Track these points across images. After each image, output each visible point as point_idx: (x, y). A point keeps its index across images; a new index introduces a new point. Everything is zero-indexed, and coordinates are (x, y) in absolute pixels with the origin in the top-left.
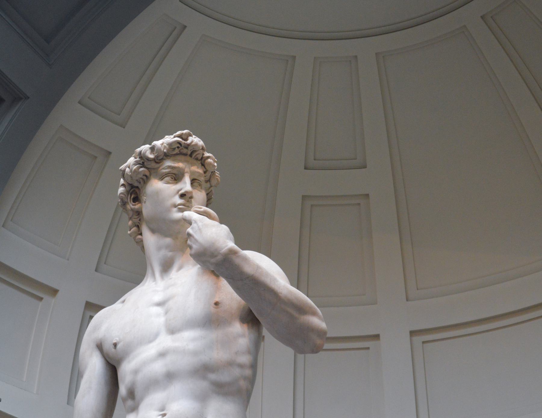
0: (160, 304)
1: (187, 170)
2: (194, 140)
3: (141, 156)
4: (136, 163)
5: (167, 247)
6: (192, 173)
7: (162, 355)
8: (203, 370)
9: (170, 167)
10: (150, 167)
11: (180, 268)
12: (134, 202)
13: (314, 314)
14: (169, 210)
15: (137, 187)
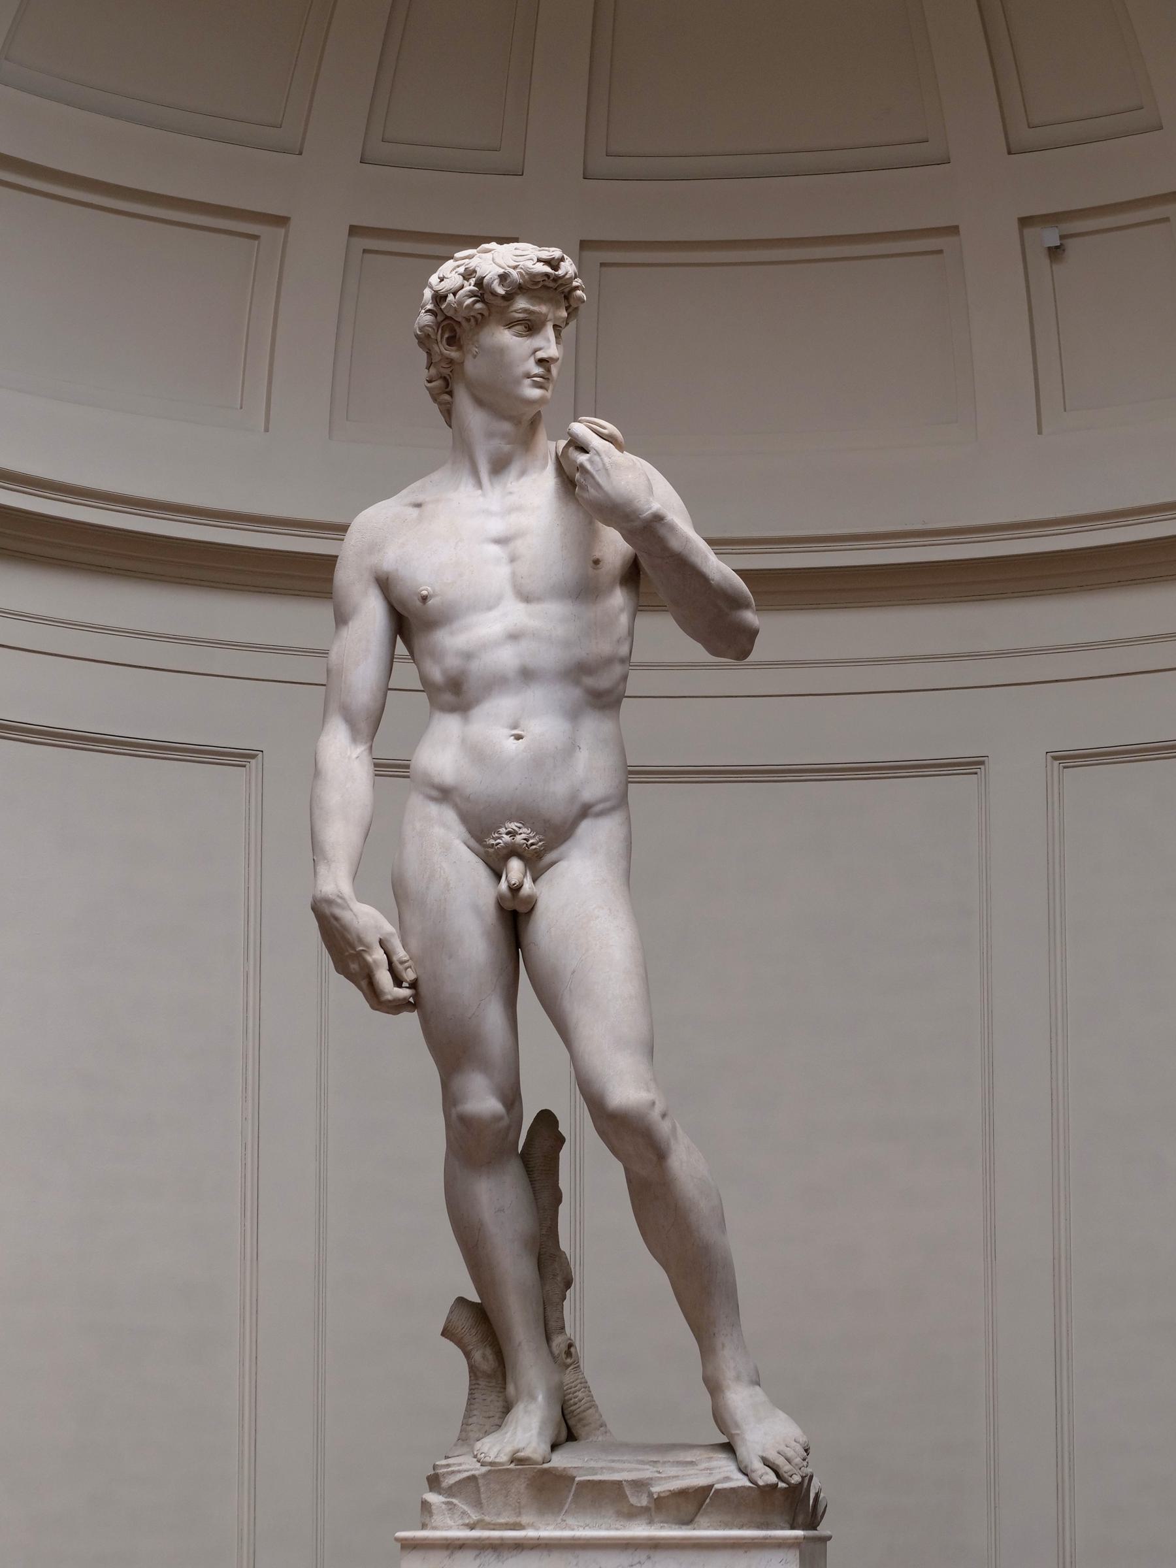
0: (501, 541)
1: (550, 316)
2: (568, 267)
3: (480, 283)
4: (472, 294)
5: (504, 436)
6: (555, 318)
7: (514, 637)
8: (578, 671)
9: (525, 311)
10: (493, 302)
11: (523, 473)
12: (449, 344)
13: (747, 606)
14: (518, 382)
15: (459, 323)
